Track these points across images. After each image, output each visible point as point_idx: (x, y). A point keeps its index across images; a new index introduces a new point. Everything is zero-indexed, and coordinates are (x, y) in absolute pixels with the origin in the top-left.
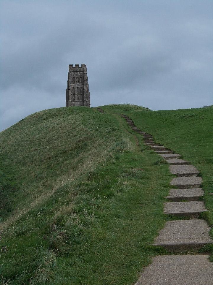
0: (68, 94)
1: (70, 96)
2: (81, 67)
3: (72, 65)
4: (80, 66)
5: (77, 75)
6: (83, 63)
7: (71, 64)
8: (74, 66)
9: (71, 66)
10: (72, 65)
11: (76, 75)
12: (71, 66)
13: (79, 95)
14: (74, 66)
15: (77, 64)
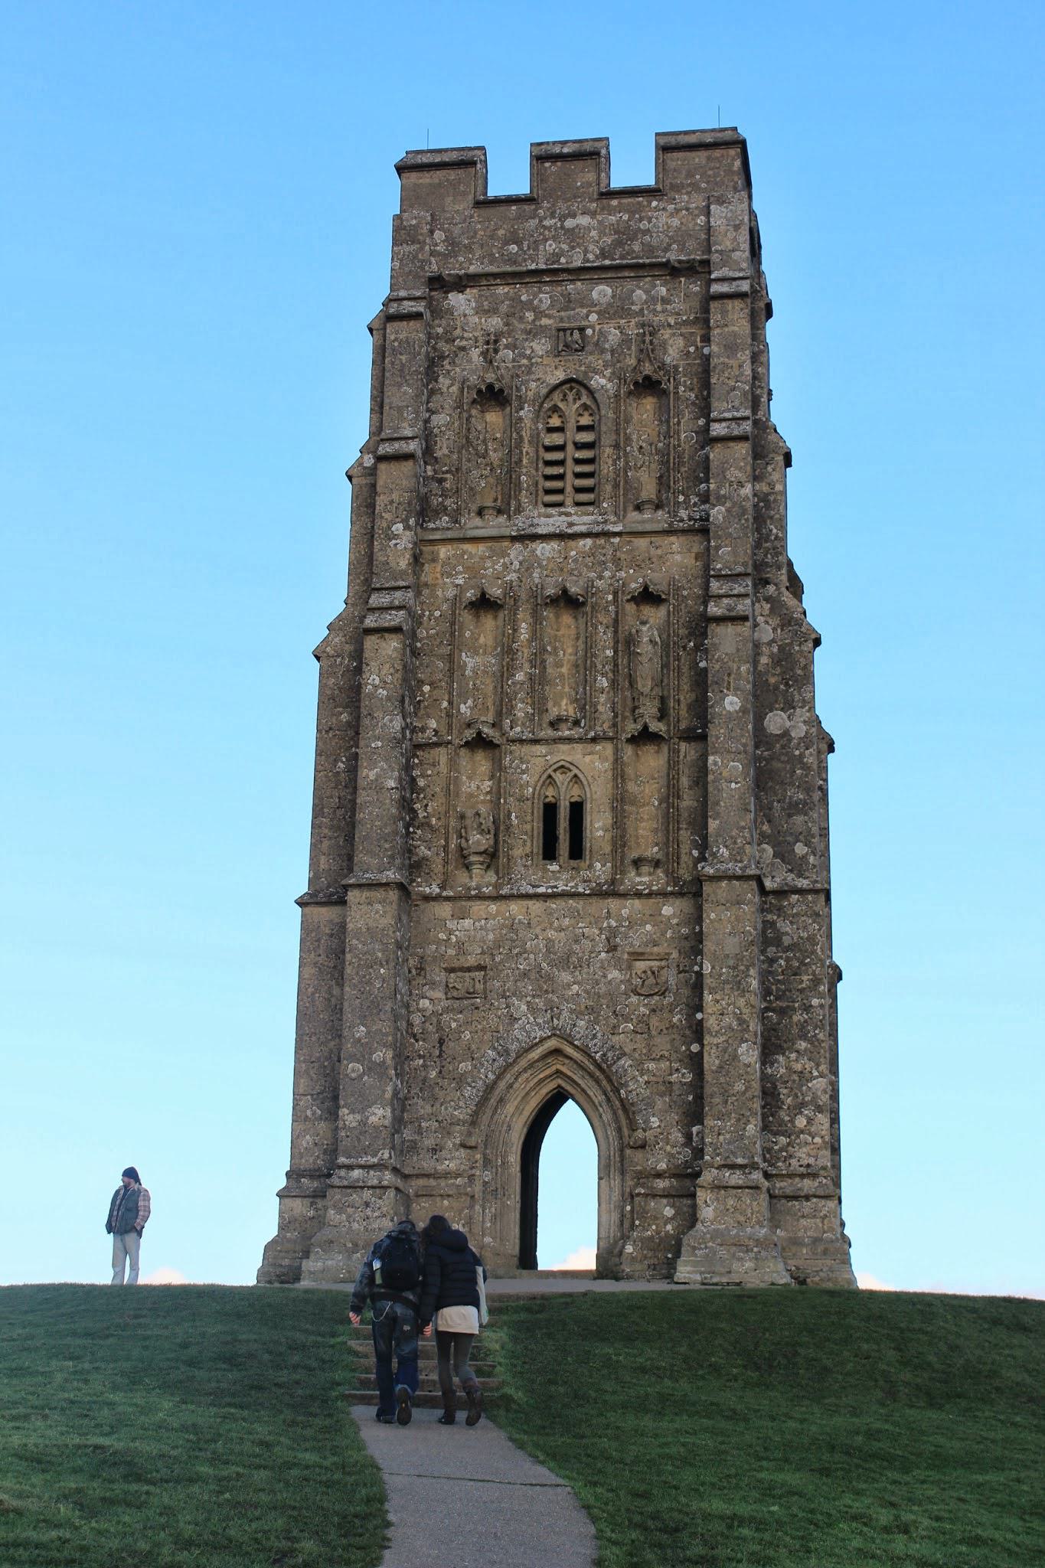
0: (355, 729)
1: (380, 774)
2: (646, 177)
3: (468, 162)
4: (632, 166)
5: (570, 341)
6: (696, 117)
7: (448, 135)
8: (509, 176)
9: (439, 175)
10: (468, 162)
11: (540, 347)
12: (439, 175)
13: (594, 764)
14: (509, 176)
15: (567, 128)
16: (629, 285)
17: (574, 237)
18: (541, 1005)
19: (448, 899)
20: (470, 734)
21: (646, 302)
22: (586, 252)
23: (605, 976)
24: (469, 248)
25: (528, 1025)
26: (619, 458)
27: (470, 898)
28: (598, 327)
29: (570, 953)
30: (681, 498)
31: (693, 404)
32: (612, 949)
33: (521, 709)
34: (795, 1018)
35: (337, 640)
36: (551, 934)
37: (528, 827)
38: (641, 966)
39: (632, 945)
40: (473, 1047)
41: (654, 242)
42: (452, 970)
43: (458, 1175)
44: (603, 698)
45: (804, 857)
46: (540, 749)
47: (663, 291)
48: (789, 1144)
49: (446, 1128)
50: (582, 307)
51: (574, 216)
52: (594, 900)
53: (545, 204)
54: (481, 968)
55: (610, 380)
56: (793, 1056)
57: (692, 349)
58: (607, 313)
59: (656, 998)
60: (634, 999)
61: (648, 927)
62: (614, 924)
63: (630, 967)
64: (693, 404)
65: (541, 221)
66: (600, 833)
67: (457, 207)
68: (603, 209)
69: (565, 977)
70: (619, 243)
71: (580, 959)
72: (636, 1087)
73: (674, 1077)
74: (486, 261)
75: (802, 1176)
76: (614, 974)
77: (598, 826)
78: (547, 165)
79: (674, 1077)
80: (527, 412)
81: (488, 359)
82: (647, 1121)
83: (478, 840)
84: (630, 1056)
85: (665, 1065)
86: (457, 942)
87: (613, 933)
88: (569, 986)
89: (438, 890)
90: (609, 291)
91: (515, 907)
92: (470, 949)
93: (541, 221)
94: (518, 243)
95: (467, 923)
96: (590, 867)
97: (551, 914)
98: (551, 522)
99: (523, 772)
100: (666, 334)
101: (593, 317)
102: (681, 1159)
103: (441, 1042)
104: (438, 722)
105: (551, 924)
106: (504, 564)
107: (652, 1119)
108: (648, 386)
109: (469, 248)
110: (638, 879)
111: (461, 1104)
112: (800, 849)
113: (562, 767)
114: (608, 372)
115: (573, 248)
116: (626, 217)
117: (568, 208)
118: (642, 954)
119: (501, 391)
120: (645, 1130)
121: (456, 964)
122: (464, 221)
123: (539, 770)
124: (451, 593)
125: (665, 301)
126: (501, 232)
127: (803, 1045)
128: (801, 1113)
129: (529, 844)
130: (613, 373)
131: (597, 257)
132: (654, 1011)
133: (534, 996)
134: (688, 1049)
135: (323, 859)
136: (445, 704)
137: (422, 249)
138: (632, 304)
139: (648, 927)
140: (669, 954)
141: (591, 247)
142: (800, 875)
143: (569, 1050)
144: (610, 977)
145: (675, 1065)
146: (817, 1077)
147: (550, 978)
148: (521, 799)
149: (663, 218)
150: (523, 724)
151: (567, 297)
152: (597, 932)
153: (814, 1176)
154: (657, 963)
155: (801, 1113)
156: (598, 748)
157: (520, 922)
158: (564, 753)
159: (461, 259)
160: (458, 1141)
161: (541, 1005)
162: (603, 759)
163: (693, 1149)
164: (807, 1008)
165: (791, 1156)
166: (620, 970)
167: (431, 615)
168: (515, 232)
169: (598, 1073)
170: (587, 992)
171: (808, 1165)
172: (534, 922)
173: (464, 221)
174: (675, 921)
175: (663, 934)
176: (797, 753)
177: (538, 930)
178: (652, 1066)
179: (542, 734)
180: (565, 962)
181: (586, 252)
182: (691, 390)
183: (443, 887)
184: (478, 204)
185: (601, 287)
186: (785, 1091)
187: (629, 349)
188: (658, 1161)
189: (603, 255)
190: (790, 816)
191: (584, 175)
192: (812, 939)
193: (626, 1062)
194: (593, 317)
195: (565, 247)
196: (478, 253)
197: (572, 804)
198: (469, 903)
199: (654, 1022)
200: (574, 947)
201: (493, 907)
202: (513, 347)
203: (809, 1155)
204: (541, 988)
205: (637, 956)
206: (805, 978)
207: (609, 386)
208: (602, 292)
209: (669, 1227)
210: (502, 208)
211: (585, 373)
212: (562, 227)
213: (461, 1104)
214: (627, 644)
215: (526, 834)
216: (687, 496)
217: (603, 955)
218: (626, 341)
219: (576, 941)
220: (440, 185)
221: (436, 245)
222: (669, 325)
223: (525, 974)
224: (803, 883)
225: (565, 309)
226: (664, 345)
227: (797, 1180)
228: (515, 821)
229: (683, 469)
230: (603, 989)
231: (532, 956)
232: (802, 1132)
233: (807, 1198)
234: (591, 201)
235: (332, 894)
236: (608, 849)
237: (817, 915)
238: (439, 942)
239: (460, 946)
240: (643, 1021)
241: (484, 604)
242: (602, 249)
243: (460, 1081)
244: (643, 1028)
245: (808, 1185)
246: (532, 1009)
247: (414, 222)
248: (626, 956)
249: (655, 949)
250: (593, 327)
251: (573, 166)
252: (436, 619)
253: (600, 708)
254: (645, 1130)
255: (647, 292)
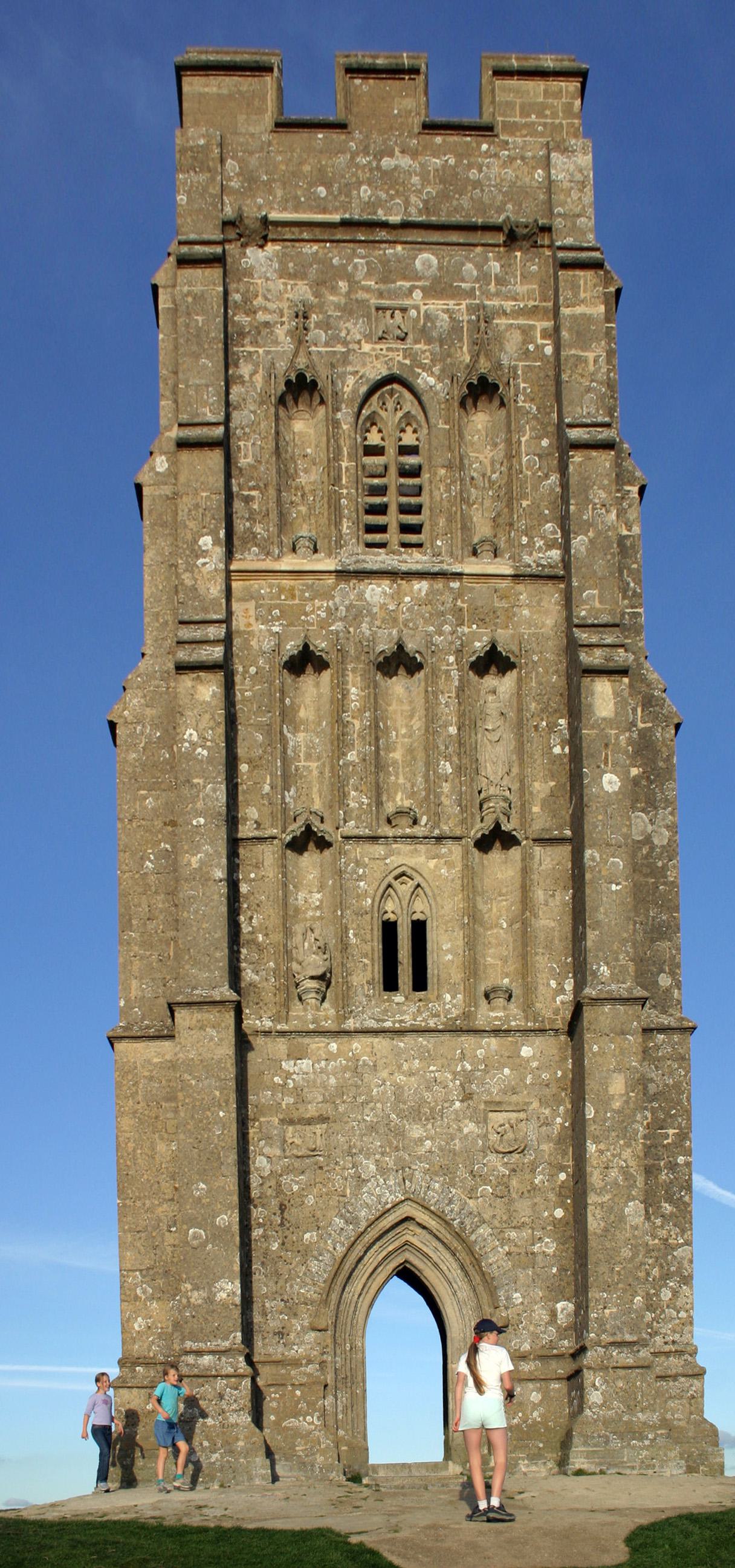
16: (459, 254)
17: (391, 179)
18: (391, 1164)
19: (282, 1033)
20: (296, 828)
21: (477, 280)
22: (407, 203)
23: (460, 1130)
24: (268, 187)
25: (382, 1191)
26: (453, 482)
27: (309, 1033)
28: (423, 308)
29: (423, 1101)
30: (525, 540)
31: (535, 417)
32: (467, 1097)
33: (358, 799)
34: (663, 1177)
35: (135, 701)
36: (400, 1078)
37: (367, 948)
38: (497, 1118)
39: (490, 1093)
40: (319, 1214)
41: (486, 199)
42: (291, 1122)
43: (310, 1362)
44: (446, 787)
45: (668, 990)
46: (379, 850)
47: (495, 267)
48: (653, 1319)
49: (291, 1309)
50: (405, 278)
51: (391, 155)
52: (446, 1037)
53: (357, 134)
54: (323, 1119)
55: (439, 379)
56: (658, 1221)
57: (531, 347)
58: (438, 288)
59: (516, 1156)
60: (492, 1157)
61: (507, 1071)
62: (469, 1067)
63: (486, 1120)
64: (535, 417)
65: (353, 158)
66: (450, 957)
67: (252, 130)
68: (425, 147)
69: (416, 1131)
70: (444, 196)
71: (432, 1109)
72: (496, 1259)
73: (536, 1248)
74: (290, 204)
75: (667, 1354)
76: (470, 1127)
77: (445, 949)
78: (358, 82)
79: (536, 1248)
80: (345, 416)
81: (300, 335)
82: (508, 1298)
83: (315, 963)
84: (490, 1224)
85: (526, 1233)
86: (295, 1088)
87: (468, 1077)
88: (421, 1141)
89: (271, 1024)
90: (434, 260)
91: (357, 1045)
92: (310, 1097)
93: (353, 158)
94: (328, 186)
95: (305, 1064)
96: (439, 997)
97: (398, 1055)
98: (379, 559)
99: (360, 878)
100: (501, 322)
101: (418, 294)
102: (545, 1339)
103: (282, 1208)
104: (259, 810)
105: (400, 1067)
106: (328, 608)
107: (516, 1295)
108: (482, 390)
109: (268, 187)
110: (493, 1014)
111: (308, 1280)
112: (664, 981)
113: (403, 874)
114: (436, 369)
115: (392, 198)
116: (452, 161)
117: (385, 142)
118: (499, 1103)
119: (314, 383)
120: (507, 1308)
121: (295, 1115)
122: (262, 149)
123: (378, 875)
124: (268, 644)
125: (500, 281)
126: (307, 168)
127: (667, 1208)
128: (666, 1285)
129: (369, 968)
130: (443, 370)
131: (420, 211)
132: (514, 1170)
133: (382, 1154)
134: (552, 1215)
135: (134, 983)
136: (267, 788)
137: (213, 179)
138: (463, 280)
139: (507, 1071)
140: (528, 1104)
141: (413, 199)
142: (664, 1012)
143: (422, 1216)
144: (466, 1130)
145: (538, 1234)
146: (682, 1245)
147: (400, 1133)
148: (360, 913)
149: (494, 170)
150: (358, 818)
151: (385, 262)
152: (450, 1076)
153: (679, 1353)
154: (515, 1115)
155: (666, 1285)
156: (443, 851)
157: (365, 1064)
158: (405, 856)
159: (260, 201)
160: (306, 1323)
161: (391, 1164)
162: (450, 865)
163: (558, 1328)
164: (673, 1167)
165: (656, 1333)
166: (477, 1123)
167: (246, 671)
168: (321, 170)
169: (456, 1244)
170: (441, 1149)
171: (674, 1342)
172: (380, 1063)
173: (262, 149)
174: (535, 1064)
175: (523, 1079)
176: (660, 864)
177: (384, 1074)
178: (513, 1234)
179: (380, 832)
180: (416, 1114)
181: (407, 203)
182: (532, 400)
183: (276, 1019)
184: (281, 125)
185: (426, 255)
186: (650, 1261)
187: (461, 340)
188: (522, 1343)
189: (427, 210)
190: (653, 941)
191: (407, 102)
192: (677, 1086)
193: (484, 1231)
194: (418, 294)
195: (384, 196)
196: (279, 193)
197: (413, 922)
198: (307, 1040)
199: (514, 1183)
200: (427, 1095)
201: (334, 1046)
202: (325, 325)
203: (674, 1331)
204: (390, 1143)
205: (496, 1106)
206: (671, 1132)
207: (439, 386)
208: (426, 260)
209: (535, 1414)
210: (304, 135)
211: (411, 368)
212: (379, 168)
213: (308, 1280)
214: (469, 722)
215: (366, 956)
216: (531, 538)
217: (458, 1104)
218: (456, 327)
219: (428, 1088)
220: (230, 96)
221: (230, 179)
222: (505, 313)
223: (372, 1128)
224: (665, 1020)
225: (385, 280)
226: (499, 339)
227: (663, 1358)
228: (353, 940)
229: (525, 503)
230: (457, 1144)
231: (379, 1105)
232: (668, 1307)
233: (675, 1377)
234: (410, 136)
235: (148, 1027)
236: (457, 976)
237: (683, 1058)
238: (274, 1087)
239: (298, 1091)
240: (503, 1182)
241: (304, 661)
242: (426, 202)
243: (305, 1252)
244: (503, 1192)
245: (674, 1364)
246: (383, 1171)
247: (202, 142)
248: (482, 1106)
249: (515, 1098)
250: (417, 308)
251: (390, 86)
252: (252, 677)
253: (446, 801)
254: (507, 1308)
255: (479, 267)
